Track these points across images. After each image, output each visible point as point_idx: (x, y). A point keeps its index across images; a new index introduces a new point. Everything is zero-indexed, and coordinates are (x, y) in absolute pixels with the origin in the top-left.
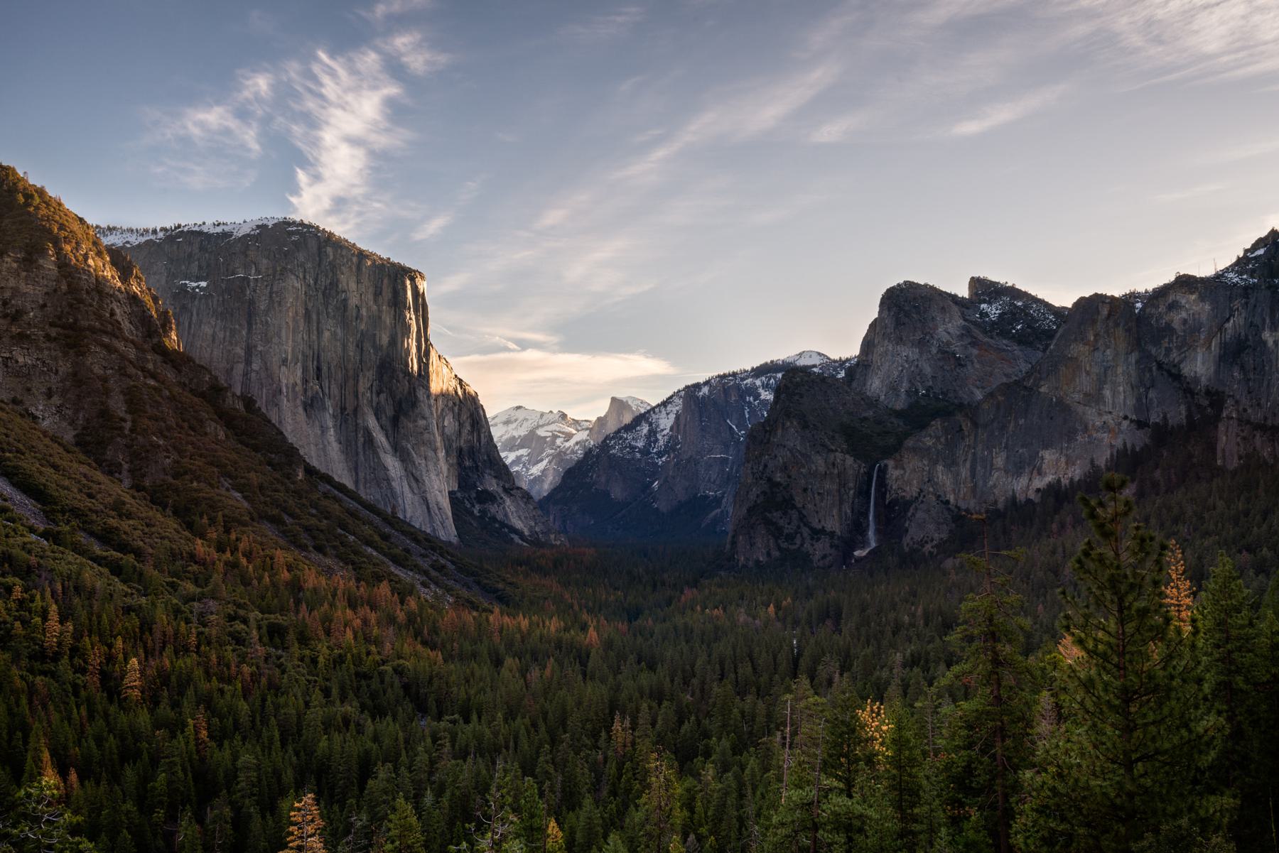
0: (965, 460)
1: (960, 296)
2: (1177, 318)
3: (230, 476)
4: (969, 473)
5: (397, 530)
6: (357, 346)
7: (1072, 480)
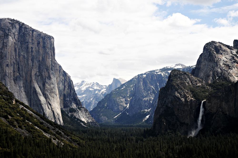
1: (230, 46)
4: (233, 104)
5: (45, 121)
6: (32, 60)
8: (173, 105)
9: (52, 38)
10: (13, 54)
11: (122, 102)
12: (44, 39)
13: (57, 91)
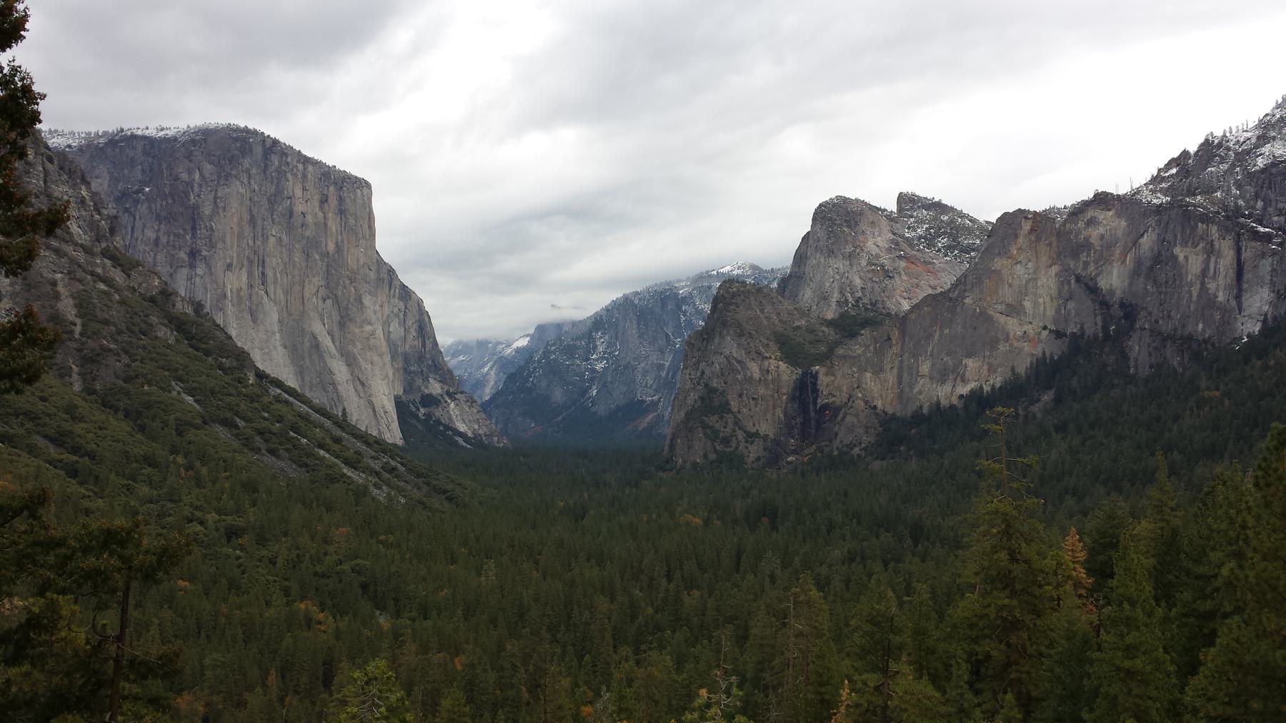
2: (1094, 234)
3: (181, 381)
4: (896, 379)
5: (347, 433)
6: (304, 252)
7: (993, 386)
8: (726, 383)
9: (364, 184)
12: (342, 187)
13: (384, 344)
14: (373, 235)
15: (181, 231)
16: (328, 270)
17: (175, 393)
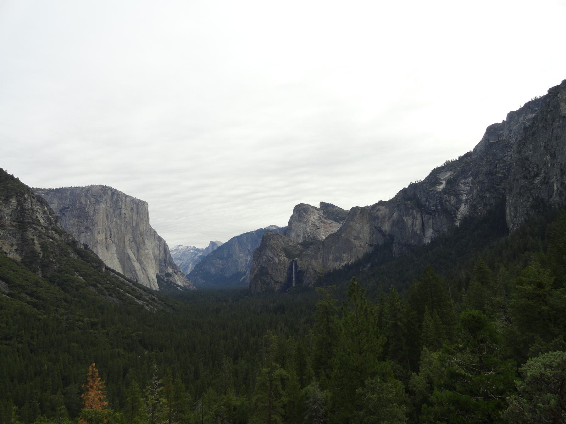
0: (321, 258)
2: (379, 213)
5: (138, 287)
6: (125, 226)
7: (352, 263)
8: (267, 265)
10: (105, 221)
11: (219, 264)
14: (148, 220)
15: (82, 221)
16: (133, 232)
17: (76, 276)
